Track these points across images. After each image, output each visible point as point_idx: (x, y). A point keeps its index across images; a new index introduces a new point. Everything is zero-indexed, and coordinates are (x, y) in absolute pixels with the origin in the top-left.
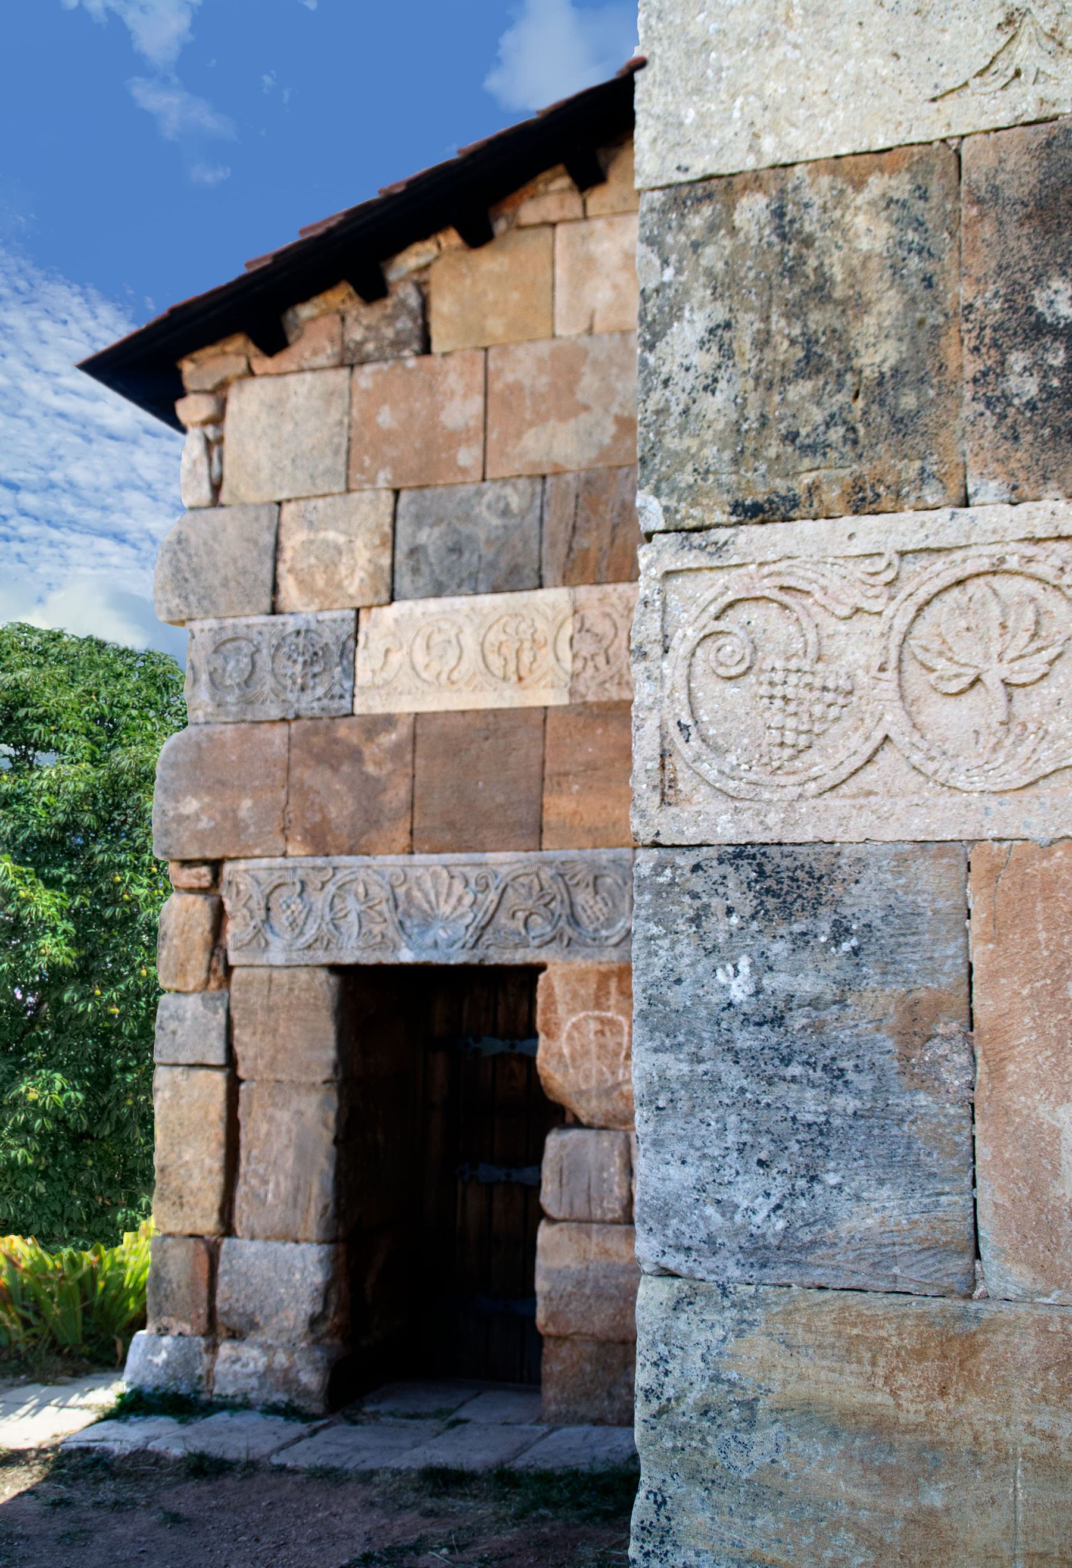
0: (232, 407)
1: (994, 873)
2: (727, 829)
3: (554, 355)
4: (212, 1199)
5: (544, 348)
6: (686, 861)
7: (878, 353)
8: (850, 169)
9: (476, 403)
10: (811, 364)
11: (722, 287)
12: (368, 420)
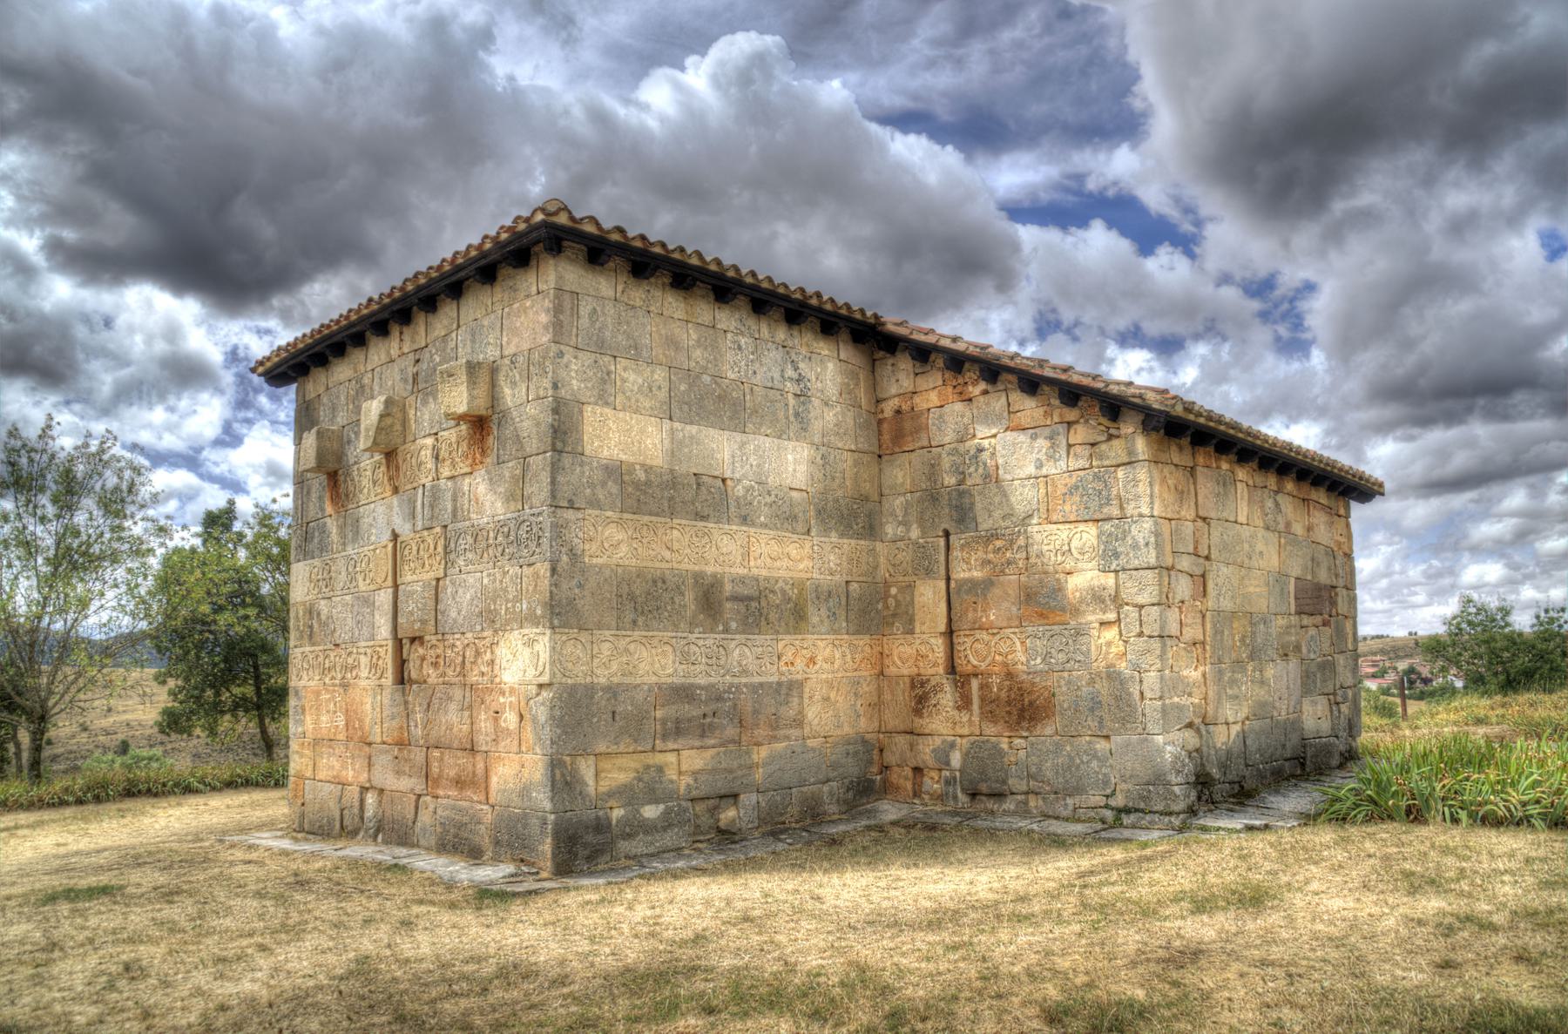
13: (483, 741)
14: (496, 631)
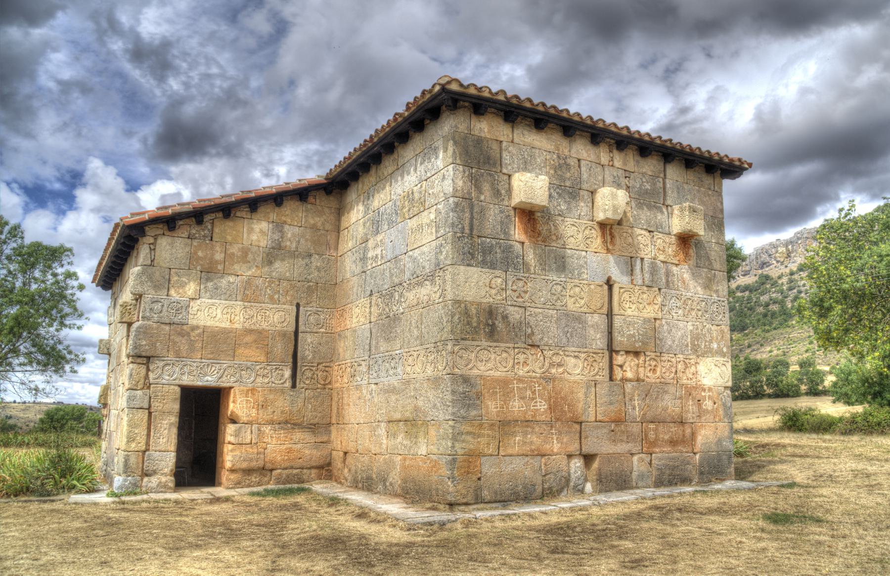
0: (159, 241)
3: (243, 248)
4: (144, 442)
5: (241, 246)
7: (475, 324)
8: (472, 303)
9: (223, 255)
11: (460, 313)
12: (196, 253)
13: (689, 417)
14: (698, 356)
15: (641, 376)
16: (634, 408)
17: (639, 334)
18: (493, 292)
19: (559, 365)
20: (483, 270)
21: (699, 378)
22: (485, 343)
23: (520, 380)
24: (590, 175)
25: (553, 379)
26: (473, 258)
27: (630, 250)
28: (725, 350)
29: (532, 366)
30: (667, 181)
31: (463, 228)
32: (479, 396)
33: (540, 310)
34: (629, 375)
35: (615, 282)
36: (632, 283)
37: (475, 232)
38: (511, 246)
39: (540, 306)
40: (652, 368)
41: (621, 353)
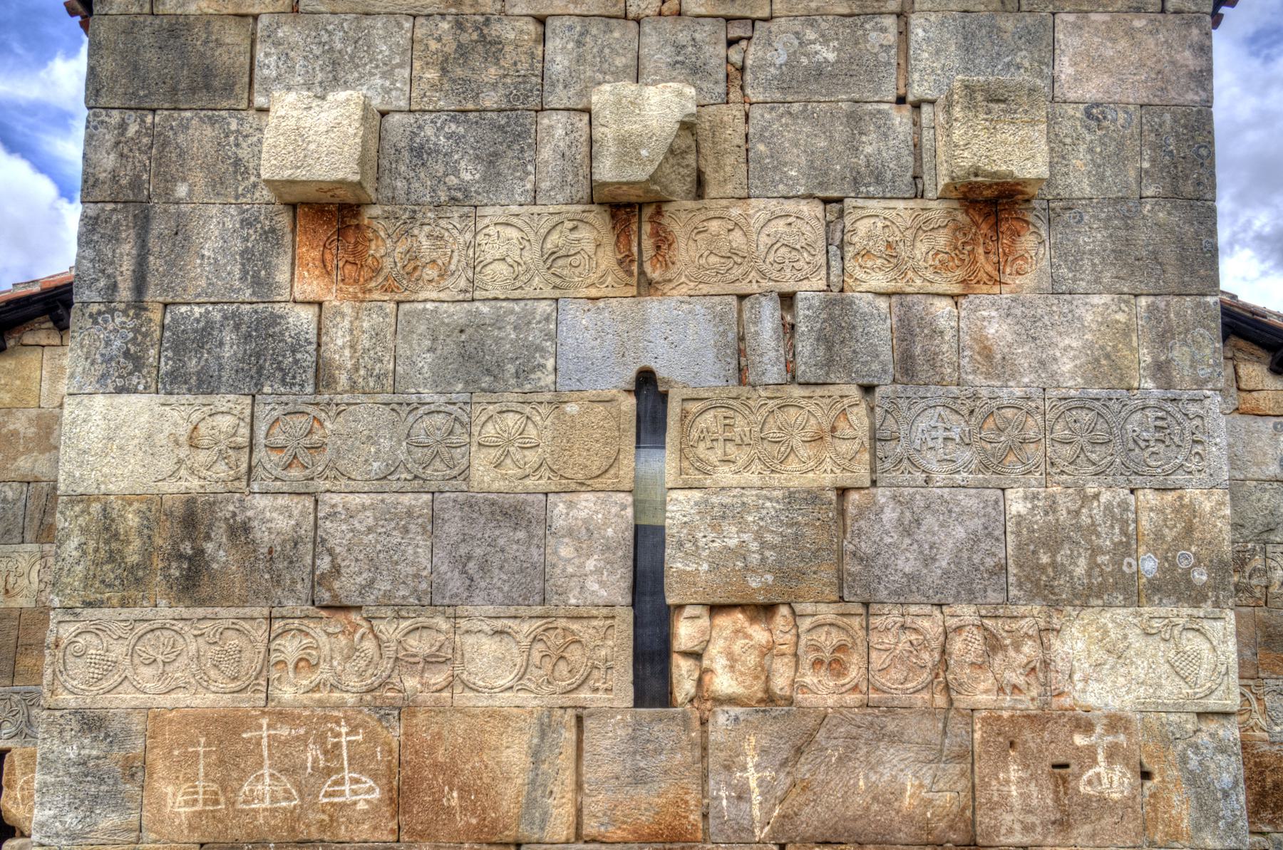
1: (155, 717)
2: (73, 704)
6: (58, 713)
7: (133, 559)
8: (127, 499)
10: (111, 559)
11: (84, 530)
14: (1055, 605)
15: (780, 683)
16: (742, 795)
17: (763, 545)
18: (202, 457)
19: (432, 661)
20: (173, 399)
21: (1058, 680)
22: (165, 612)
23: (282, 716)
24: (580, 60)
25: (406, 709)
26: (138, 368)
27: (737, 272)
28: (1200, 576)
29: (322, 667)
30: (915, 20)
31: (114, 287)
32: (136, 770)
33: (366, 499)
34: (723, 683)
35: (667, 382)
36: (741, 382)
37: (153, 296)
38: (275, 319)
39: (359, 486)
40: (827, 655)
41: (688, 611)
